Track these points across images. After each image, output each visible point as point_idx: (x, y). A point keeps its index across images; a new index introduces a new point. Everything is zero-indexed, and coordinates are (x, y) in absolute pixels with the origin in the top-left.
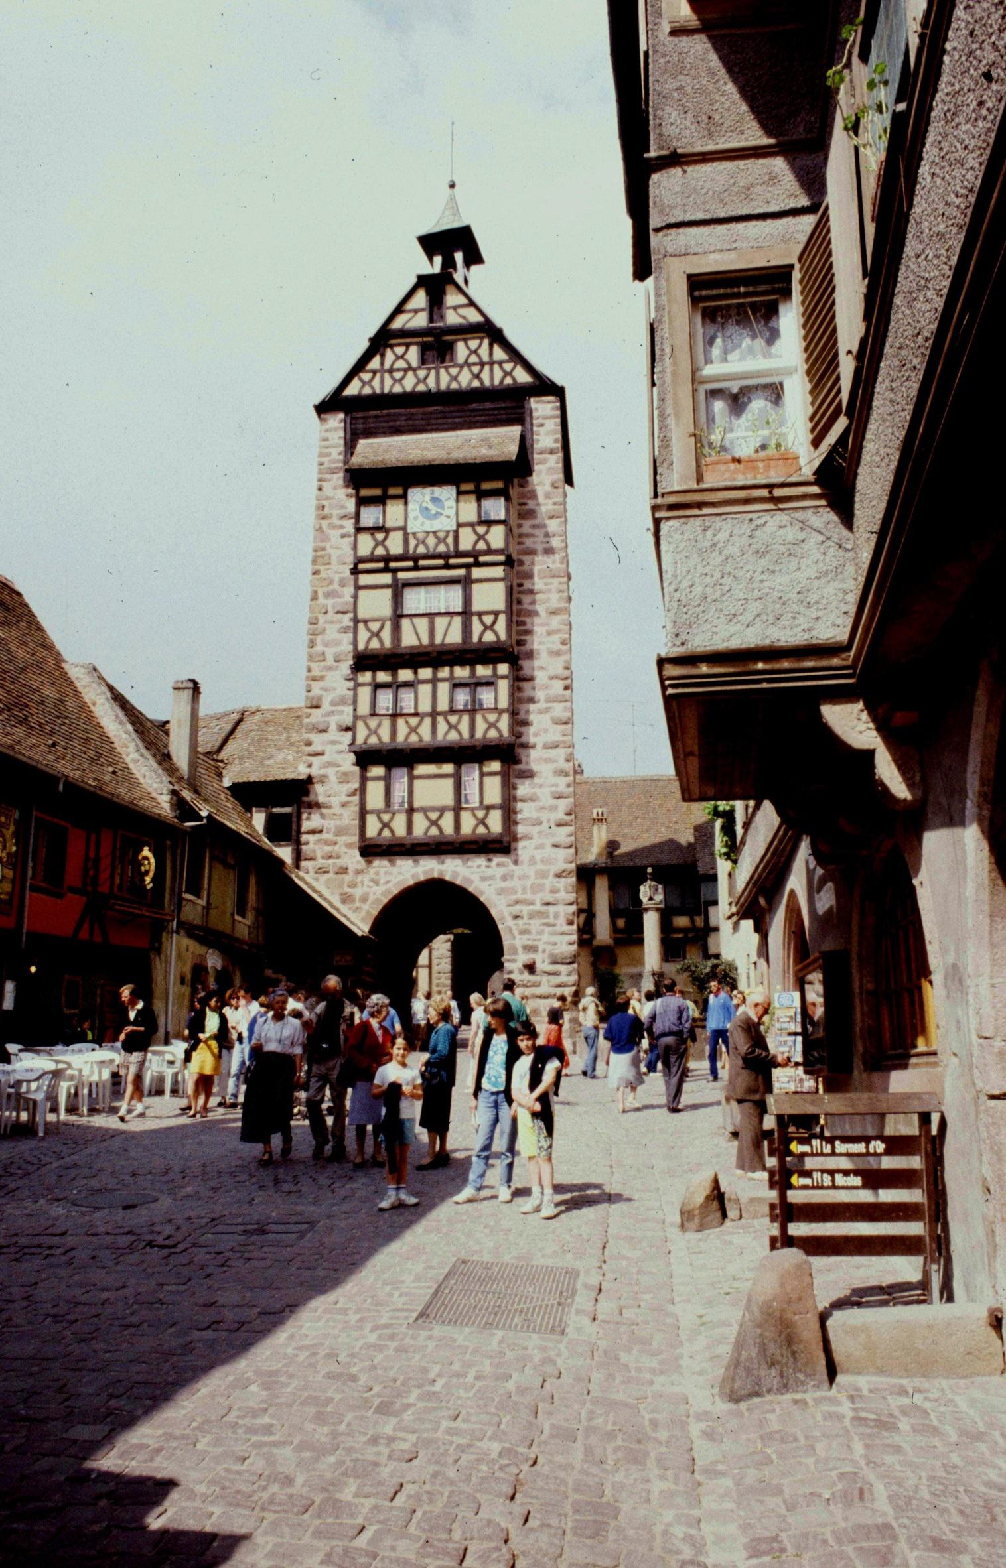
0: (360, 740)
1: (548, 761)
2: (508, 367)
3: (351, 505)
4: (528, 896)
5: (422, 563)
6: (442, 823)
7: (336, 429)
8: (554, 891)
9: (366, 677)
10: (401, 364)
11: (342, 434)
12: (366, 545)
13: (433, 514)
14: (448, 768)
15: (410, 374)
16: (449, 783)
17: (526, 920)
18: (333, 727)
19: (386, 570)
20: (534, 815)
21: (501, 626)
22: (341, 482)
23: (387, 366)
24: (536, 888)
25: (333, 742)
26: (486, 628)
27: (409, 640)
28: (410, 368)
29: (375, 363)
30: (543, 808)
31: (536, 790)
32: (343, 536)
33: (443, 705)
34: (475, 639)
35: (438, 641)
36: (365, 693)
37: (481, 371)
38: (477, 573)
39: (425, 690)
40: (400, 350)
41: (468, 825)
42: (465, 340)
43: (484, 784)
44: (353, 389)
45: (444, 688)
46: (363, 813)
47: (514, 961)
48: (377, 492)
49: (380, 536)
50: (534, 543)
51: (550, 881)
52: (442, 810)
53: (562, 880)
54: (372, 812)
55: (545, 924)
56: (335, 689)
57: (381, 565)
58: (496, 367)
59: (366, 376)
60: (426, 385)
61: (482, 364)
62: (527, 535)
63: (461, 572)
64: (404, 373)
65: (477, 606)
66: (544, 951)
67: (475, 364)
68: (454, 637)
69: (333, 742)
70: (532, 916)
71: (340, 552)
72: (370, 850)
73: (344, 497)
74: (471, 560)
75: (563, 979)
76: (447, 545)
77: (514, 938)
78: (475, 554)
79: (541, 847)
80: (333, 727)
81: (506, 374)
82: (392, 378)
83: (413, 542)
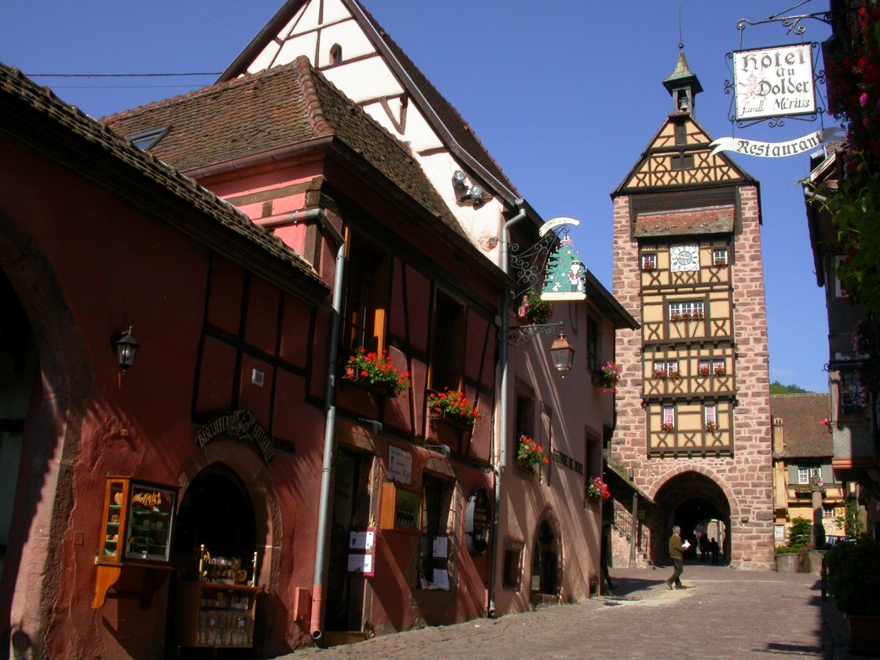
0: (647, 392)
1: (755, 404)
2: (725, 169)
3: (635, 253)
4: (744, 481)
5: (680, 290)
6: (694, 439)
7: (623, 207)
8: (759, 478)
9: (648, 355)
10: (661, 168)
11: (627, 210)
12: (647, 279)
13: (686, 260)
14: (697, 408)
15: (667, 174)
16: (698, 417)
17: (743, 495)
18: (629, 382)
19: (659, 294)
20: (747, 435)
21: (727, 327)
22: (629, 239)
23: (653, 169)
24: (748, 477)
25: (629, 392)
26: (719, 328)
27: (674, 334)
28: (666, 170)
29: (645, 168)
30: (753, 431)
31: (749, 421)
32: (631, 271)
33: (694, 372)
34: (713, 334)
35: (691, 335)
36: (648, 365)
37: (709, 172)
38: (713, 296)
39: (683, 364)
40: (660, 160)
41: (710, 440)
42: (699, 154)
43: (716, 414)
44: (633, 183)
45: (694, 363)
46: (649, 433)
47: (737, 518)
48: (651, 250)
49: (655, 274)
50: (745, 275)
51: (757, 474)
52: (694, 432)
53: (765, 473)
54: (654, 433)
55: (753, 498)
56: (629, 361)
57: (656, 291)
58: (718, 170)
59: (641, 176)
60: (677, 181)
61: (709, 168)
62: (740, 271)
63: (703, 295)
64: (661, 173)
65: (713, 316)
66: (754, 512)
67: (705, 168)
68: (700, 333)
69: (629, 392)
70: (747, 492)
71: (629, 280)
72: (652, 453)
73: (630, 248)
74: (708, 288)
75: (765, 527)
76: (694, 279)
77: (737, 505)
78: (710, 284)
79: (751, 453)
80: (629, 382)
81: (724, 174)
82: (656, 176)
83: (674, 278)
